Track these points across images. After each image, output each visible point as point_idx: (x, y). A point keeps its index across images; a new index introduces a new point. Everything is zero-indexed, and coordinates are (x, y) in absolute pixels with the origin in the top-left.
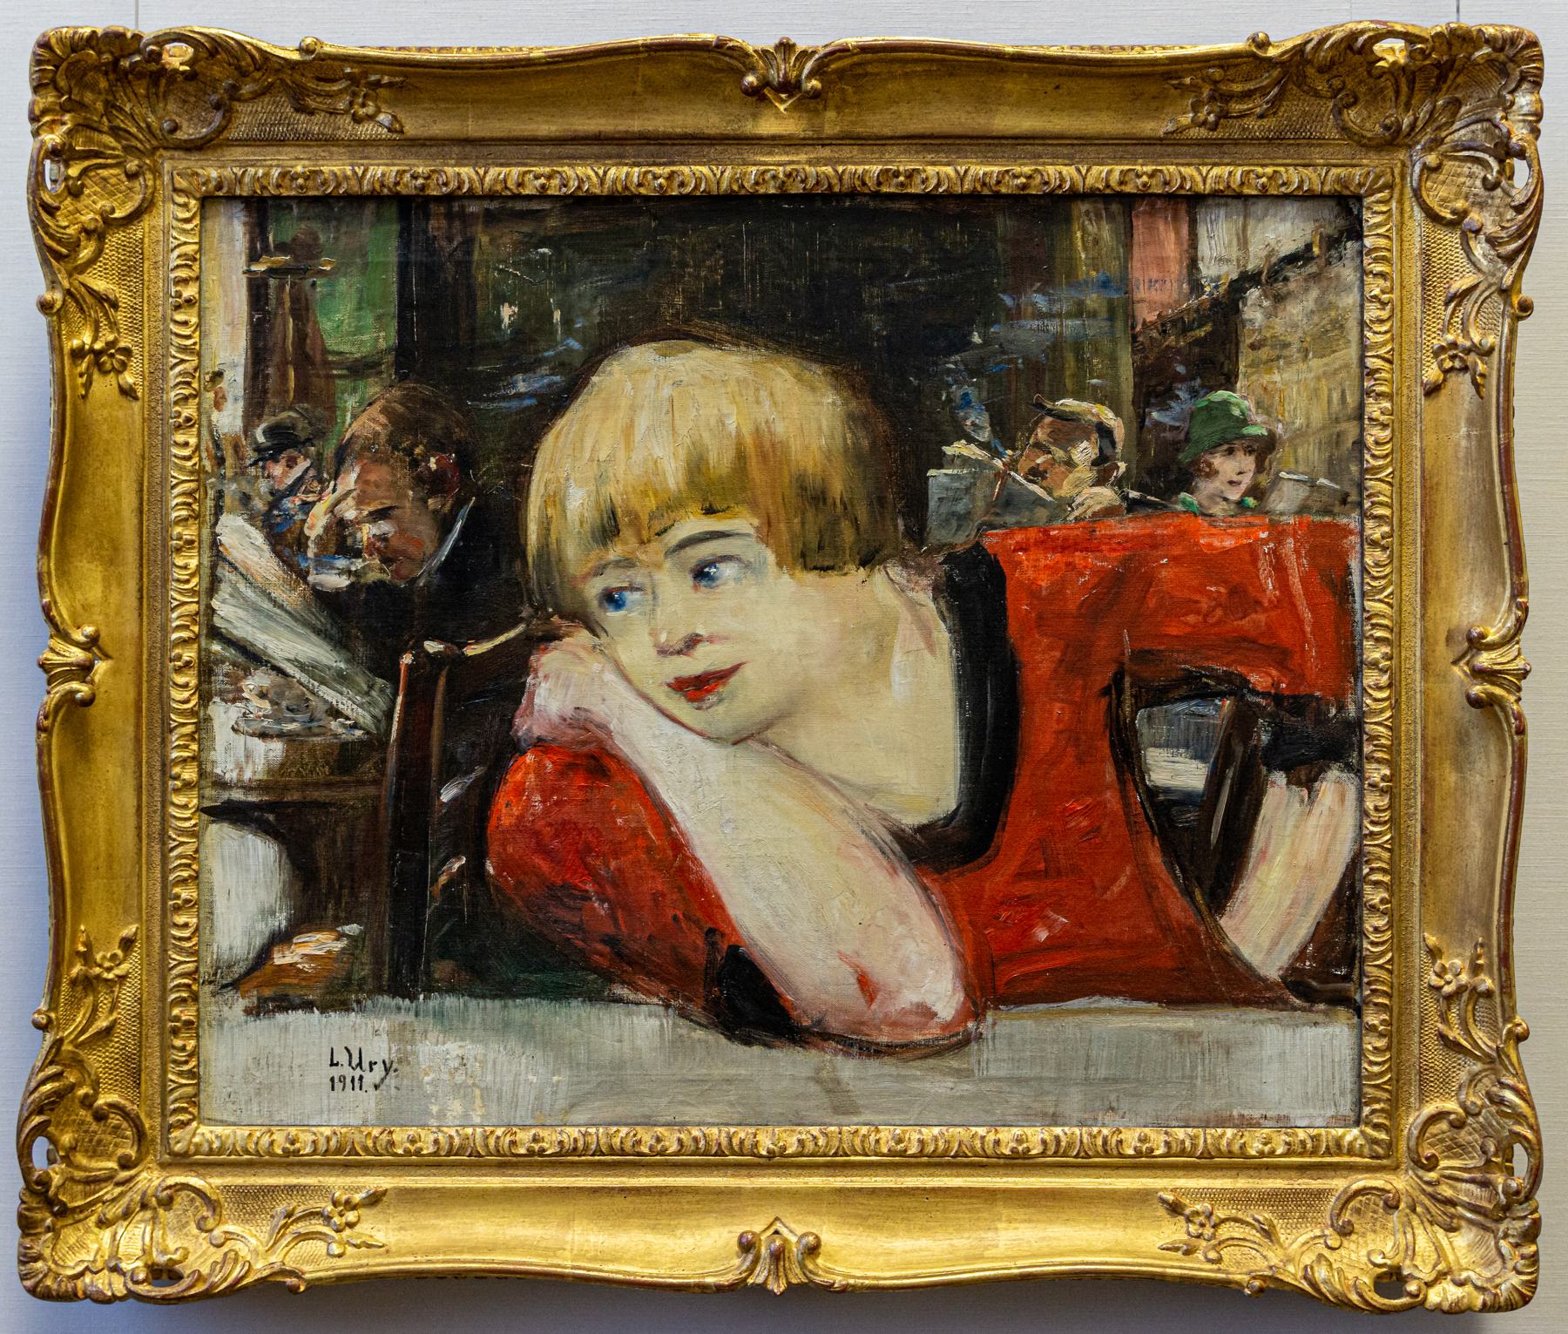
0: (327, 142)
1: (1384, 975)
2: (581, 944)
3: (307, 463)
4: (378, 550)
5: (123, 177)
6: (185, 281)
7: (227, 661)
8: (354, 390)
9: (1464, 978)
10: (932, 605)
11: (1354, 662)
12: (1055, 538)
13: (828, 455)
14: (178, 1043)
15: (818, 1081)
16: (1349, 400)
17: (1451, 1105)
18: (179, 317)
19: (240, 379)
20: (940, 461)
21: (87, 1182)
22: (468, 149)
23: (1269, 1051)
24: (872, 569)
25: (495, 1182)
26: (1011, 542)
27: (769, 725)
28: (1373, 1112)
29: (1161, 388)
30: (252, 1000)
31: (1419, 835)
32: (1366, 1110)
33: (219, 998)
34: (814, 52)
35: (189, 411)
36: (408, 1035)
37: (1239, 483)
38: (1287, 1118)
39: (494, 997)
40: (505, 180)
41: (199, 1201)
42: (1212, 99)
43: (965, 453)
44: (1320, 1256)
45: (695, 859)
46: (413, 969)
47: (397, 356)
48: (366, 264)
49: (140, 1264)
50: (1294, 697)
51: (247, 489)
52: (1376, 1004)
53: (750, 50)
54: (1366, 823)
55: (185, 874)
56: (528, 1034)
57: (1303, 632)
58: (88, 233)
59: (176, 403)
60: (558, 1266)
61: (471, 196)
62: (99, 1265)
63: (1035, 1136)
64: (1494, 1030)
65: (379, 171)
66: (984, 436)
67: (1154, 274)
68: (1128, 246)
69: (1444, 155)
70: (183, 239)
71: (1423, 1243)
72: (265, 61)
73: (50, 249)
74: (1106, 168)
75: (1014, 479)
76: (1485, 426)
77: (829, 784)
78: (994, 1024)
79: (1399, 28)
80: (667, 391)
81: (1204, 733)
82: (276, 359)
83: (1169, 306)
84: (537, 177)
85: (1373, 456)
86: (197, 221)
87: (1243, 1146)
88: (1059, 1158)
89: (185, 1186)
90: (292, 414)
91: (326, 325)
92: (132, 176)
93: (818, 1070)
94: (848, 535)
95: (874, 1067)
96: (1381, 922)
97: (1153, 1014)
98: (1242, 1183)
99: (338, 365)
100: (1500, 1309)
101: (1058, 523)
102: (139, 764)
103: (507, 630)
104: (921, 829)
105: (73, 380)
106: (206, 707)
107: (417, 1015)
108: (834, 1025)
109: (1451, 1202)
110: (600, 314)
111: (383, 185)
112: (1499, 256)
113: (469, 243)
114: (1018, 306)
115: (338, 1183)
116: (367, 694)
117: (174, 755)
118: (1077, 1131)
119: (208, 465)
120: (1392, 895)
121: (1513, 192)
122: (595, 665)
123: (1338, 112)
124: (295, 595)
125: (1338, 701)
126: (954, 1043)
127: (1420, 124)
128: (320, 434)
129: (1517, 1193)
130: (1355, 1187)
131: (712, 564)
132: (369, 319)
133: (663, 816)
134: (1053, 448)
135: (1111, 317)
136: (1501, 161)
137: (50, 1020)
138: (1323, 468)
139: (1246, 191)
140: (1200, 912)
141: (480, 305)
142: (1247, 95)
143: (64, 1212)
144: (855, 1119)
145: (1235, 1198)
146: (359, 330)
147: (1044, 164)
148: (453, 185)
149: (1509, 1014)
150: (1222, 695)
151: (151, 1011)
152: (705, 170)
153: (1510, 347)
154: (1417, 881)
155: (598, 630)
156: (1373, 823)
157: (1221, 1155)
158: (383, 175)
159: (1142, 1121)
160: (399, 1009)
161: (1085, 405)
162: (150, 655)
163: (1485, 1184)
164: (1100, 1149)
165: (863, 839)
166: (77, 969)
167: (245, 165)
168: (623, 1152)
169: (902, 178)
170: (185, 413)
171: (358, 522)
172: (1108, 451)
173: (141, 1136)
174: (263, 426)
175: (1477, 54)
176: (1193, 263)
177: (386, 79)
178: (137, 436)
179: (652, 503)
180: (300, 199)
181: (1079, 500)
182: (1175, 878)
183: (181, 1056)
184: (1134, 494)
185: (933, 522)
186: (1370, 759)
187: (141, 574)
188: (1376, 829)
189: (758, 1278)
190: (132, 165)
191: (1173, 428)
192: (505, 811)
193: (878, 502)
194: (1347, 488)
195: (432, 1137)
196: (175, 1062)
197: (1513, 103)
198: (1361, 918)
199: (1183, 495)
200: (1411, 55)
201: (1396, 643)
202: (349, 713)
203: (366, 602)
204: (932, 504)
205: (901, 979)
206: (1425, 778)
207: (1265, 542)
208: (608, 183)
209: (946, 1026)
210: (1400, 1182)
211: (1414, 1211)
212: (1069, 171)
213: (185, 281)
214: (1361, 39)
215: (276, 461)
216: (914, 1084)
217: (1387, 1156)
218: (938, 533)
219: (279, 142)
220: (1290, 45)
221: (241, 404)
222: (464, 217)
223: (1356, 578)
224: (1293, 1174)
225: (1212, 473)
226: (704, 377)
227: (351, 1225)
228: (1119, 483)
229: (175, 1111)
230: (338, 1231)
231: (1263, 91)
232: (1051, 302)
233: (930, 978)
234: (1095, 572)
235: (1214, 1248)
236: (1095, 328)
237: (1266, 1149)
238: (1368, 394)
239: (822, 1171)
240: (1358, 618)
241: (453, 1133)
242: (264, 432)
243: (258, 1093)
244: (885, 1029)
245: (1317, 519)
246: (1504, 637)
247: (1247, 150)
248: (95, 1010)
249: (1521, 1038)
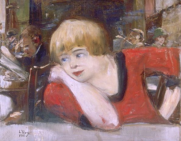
2: (59, 114)
3: (15, 38)
10: (114, 61)
26: (126, 51)
29: (150, 27)
43: (119, 37)
45: (77, 101)
46: (32, 118)
50: (171, 76)
66: (122, 34)
77: (97, 89)
80: (72, 27)
91: (18, 16)
94: (101, 50)
97: (148, 125)
101: (134, 48)
103: (47, 64)
104: (112, 96)
108: (99, 127)
114: (127, 14)
124: (13, 59)
126: (117, 130)
131: (79, 54)
133: (72, 94)
135: (142, 16)
141: (42, 13)
146: (24, 17)
150: (159, 75)
161: (138, 30)
171: (23, 47)
176: (155, 8)
181: (137, 44)
184: (146, 44)
185: (114, 48)
192: (47, 93)
199: (153, 44)
203: (24, 60)
207: (166, 51)
221: (5, 29)
233: (113, 119)
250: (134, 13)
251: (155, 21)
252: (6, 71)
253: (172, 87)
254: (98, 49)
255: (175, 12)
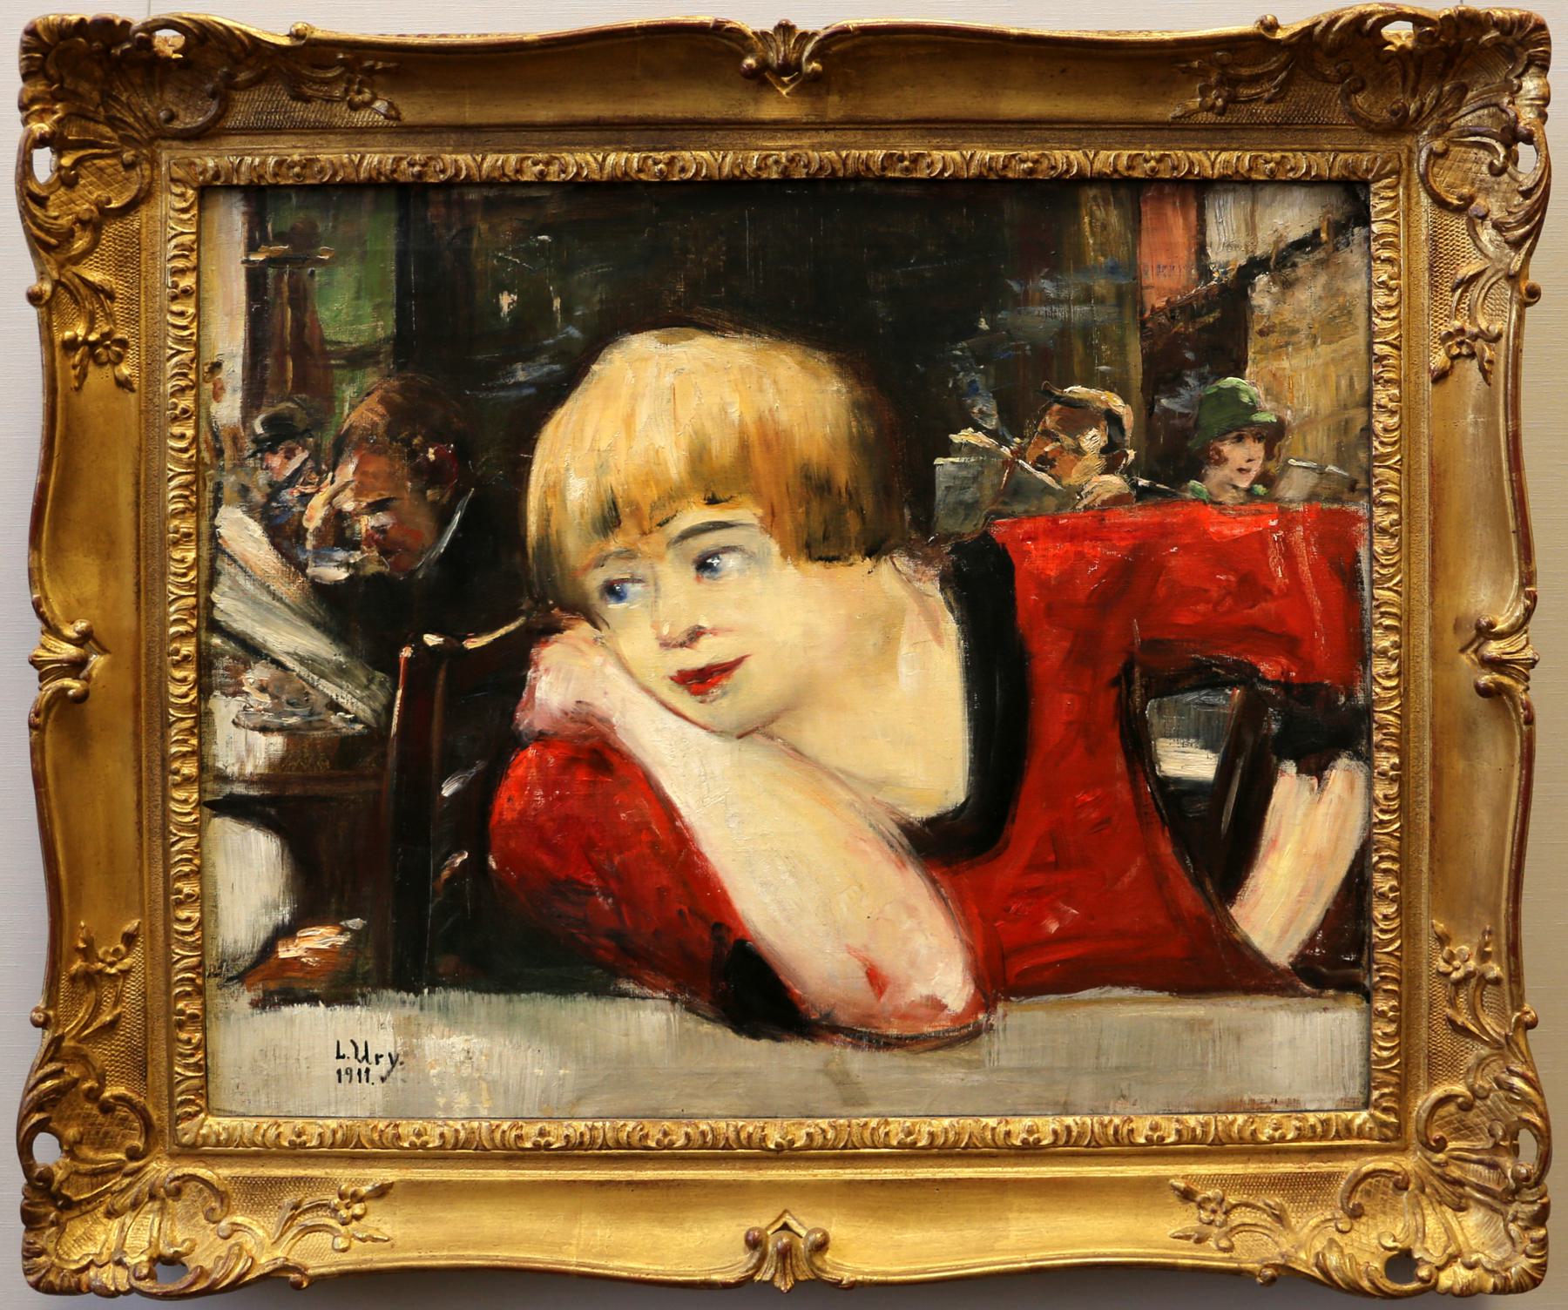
0: (325, 130)
1: (1393, 962)
2: (584, 939)
3: (305, 455)
4: (377, 542)
5: (121, 168)
6: (182, 272)
7: (222, 655)
8: (352, 380)
9: (1472, 964)
11: (1363, 650)
12: (1064, 527)
13: (833, 443)
14: (184, 1036)
15: (826, 1072)
16: (1357, 386)
17: (1459, 1088)
18: (176, 308)
19: (239, 370)
20: (947, 449)
21: (94, 1174)
22: (466, 136)
23: (1279, 1036)
24: (878, 560)
25: (501, 1174)
26: (1020, 532)
27: (774, 718)
28: (1383, 1096)
29: (1169, 375)
30: (257, 994)
31: (1427, 822)
32: (1376, 1094)
33: (225, 990)
34: (814, 34)
35: (186, 402)
36: (414, 1028)
37: (1248, 471)
38: (1296, 1101)
39: (498, 992)
40: (503, 167)
41: (207, 1193)
42: (1220, 83)
43: (973, 441)
44: (1332, 1241)
45: (700, 854)
47: (395, 345)
48: (365, 253)
49: (144, 1258)
50: (1303, 685)
51: (246, 481)
52: (1386, 991)
53: (749, 31)
54: (1375, 811)
55: (187, 869)
56: (535, 1029)
57: (1313, 621)
58: (84, 224)
59: (173, 395)
60: (563, 1263)
61: (469, 182)
62: (105, 1258)
63: (1048, 1127)
64: (1502, 1016)
65: (375, 159)
66: (992, 423)
67: (1163, 260)
68: (1136, 229)
69: (1451, 141)
70: (180, 229)
71: (1432, 1223)
72: (254, 47)
73: (38, 239)
74: (1114, 153)
75: (1022, 467)
76: (1493, 412)
78: (1005, 1015)
79: (1408, 10)
80: (668, 379)
81: (1215, 723)
82: (275, 349)
83: (1178, 292)
84: (535, 164)
85: (1382, 443)
86: (194, 211)
87: (1254, 1132)
88: (1069, 1147)
89: (194, 1177)
90: (290, 404)
91: (324, 314)
92: (129, 166)
93: (827, 1063)
94: (853, 525)
95: (884, 1059)
96: (1390, 910)
97: (1163, 1003)
98: (1253, 1168)
99: (337, 355)
100: (1511, 1292)
102: (139, 760)
104: (930, 822)
105: (65, 371)
106: (207, 700)
107: (422, 1008)
108: (843, 1018)
109: (1459, 1183)
110: (601, 301)
111: (379, 173)
112: (1507, 242)
113: (467, 231)
114: (1026, 292)
115: (345, 1175)
116: (367, 687)
117: (174, 749)
118: (1088, 1120)
119: (206, 456)
120: (1400, 883)
121: (1521, 178)
122: (597, 658)
123: (1346, 96)
124: (294, 588)
125: (1347, 688)
127: (1427, 110)
128: (318, 425)
129: (1527, 1178)
130: (1365, 1169)
131: (715, 555)
132: (367, 308)
133: (668, 811)
134: (1061, 436)
136: (1508, 146)
137: (47, 1018)
138: (1331, 455)
139: (1255, 176)
140: (1210, 902)
142: (1254, 80)
143: (69, 1205)
144: (865, 1111)
145: (1246, 1183)
146: (358, 319)
147: (1051, 149)
148: (451, 172)
149: (1518, 1002)
151: (158, 1003)
152: (706, 155)
153: (1518, 334)
154: (1425, 868)
155: (600, 623)
156: (1383, 811)
157: (1232, 1140)
158: (380, 162)
159: (1153, 1109)
160: (404, 1002)
161: (1093, 391)
162: (149, 649)
163: (1493, 1166)
164: (1111, 1138)
165: (871, 834)
166: (78, 965)
167: (242, 154)
168: (630, 1146)
169: (906, 163)
170: (182, 405)
171: (355, 514)
172: (1117, 439)
173: (148, 1127)
174: (261, 417)
175: (1485, 38)
176: (1201, 249)
177: (380, 65)
178: (134, 429)
179: (653, 494)
180: (300, 188)
181: (1088, 488)
182: (1186, 868)
183: (187, 1049)
184: (1143, 482)
186: (1379, 747)
187: (138, 568)
188: (1386, 817)
189: (765, 1275)
190: (128, 156)
191: (1182, 415)
192: (507, 805)
193: (885, 492)
194: (1356, 475)
195: (438, 1131)
196: (181, 1055)
197: (1520, 87)
198: (1370, 904)
199: (1193, 483)
200: (1419, 38)
201: (1405, 631)
202: (348, 706)
204: (939, 493)
205: (911, 972)
206: (1434, 766)
207: (1275, 529)
208: (608, 169)
209: (956, 1018)
210: (1408, 1163)
211: (1423, 1191)
212: (1076, 156)
213: (182, 272)
214: (1370, 22)
215: (275, 453)
216: (925, 1076)
217: (1397, 1139)
218: (946, 522)
219: (275, 131)
220: (1298, 27)
221: (239, 395)
222: (463, 204)
223: (1364, 566)
224: (1303, 1157)
225: (1222, 461)
226: (707, 365)
227: (357, 1218)
228: (1128, 472)
229: (183, 1103)
230: (343, 1224)
231: (1271, 76)
232: (1058, 287)
234: (1106, 560)
235: (1226, 1235)
236: (1102, 314)
237: (1277, 1134)
238: (1377, 381)
239: (831, 1163)
240: (1367, 605)
241: (459, 1127)
242: (263, 424)
243: (266, 1084)
244: (895, 1021)
245: (1326, 506)
246: (1512, 626)
247: (1255, 135)
248: (98, 1005)
249: (1532, 1025)
250: (1073, 285)
251: (1205, 336)
252: (247, 667)
253: (1313, 763)
254: (840, 518)
255: (1332, 278)
